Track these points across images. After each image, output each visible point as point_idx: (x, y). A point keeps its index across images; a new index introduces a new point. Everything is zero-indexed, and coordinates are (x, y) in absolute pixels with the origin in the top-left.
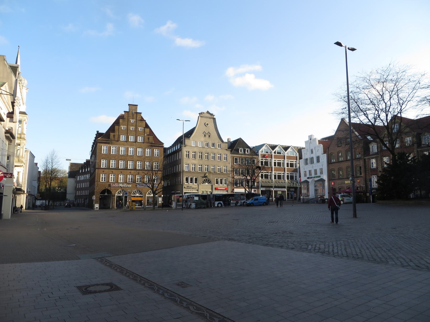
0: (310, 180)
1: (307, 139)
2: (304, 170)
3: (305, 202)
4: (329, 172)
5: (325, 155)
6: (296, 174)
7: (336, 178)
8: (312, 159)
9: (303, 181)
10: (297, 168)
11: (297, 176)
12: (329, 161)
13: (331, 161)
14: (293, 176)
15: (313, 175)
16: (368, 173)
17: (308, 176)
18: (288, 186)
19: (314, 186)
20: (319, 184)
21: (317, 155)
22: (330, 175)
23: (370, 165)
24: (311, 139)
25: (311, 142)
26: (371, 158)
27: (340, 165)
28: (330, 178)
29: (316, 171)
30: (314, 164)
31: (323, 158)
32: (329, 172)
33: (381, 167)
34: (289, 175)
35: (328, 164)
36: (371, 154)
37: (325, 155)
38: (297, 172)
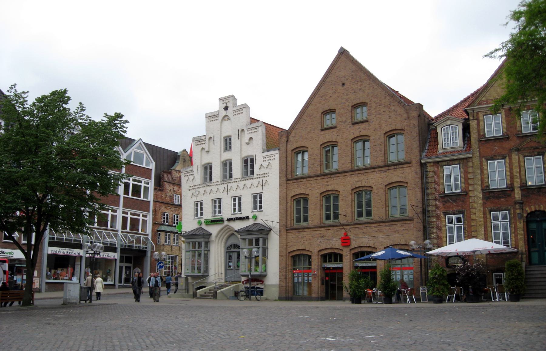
0: (214, 230)
1: (215, 107)
2: (194, 199)
3: (201, 295)
4: (287, 203)
5: (276, 155)
6: (146, 216)
7: (310, 223)
8: (227, 165)
9: (277, 214)
10: (149, 200)
11: (146, 221)
12: (289, 173)
13: (293, 171)
14: (139, 219)
15: (227, 212)
16: (434, 208)
17: (208, 214)
18: (126, 246)
19: (225, 246)
20: (245, 239)
21: (245, 154)
22: (289, 212)
23: (441, 182)
24: (226, 108)
25: (226, 116)
26: (444, 164)
27: (329, 183)
28: (289, 223)
29: (237, 201)
30: (233, 180)
31: (265, 164)
32: (287, 203)
33: (482, 190)
34: (127, 218)
35: (285, 182)
36: (440, 152)
37: (276, 155)
38: (149, 211)
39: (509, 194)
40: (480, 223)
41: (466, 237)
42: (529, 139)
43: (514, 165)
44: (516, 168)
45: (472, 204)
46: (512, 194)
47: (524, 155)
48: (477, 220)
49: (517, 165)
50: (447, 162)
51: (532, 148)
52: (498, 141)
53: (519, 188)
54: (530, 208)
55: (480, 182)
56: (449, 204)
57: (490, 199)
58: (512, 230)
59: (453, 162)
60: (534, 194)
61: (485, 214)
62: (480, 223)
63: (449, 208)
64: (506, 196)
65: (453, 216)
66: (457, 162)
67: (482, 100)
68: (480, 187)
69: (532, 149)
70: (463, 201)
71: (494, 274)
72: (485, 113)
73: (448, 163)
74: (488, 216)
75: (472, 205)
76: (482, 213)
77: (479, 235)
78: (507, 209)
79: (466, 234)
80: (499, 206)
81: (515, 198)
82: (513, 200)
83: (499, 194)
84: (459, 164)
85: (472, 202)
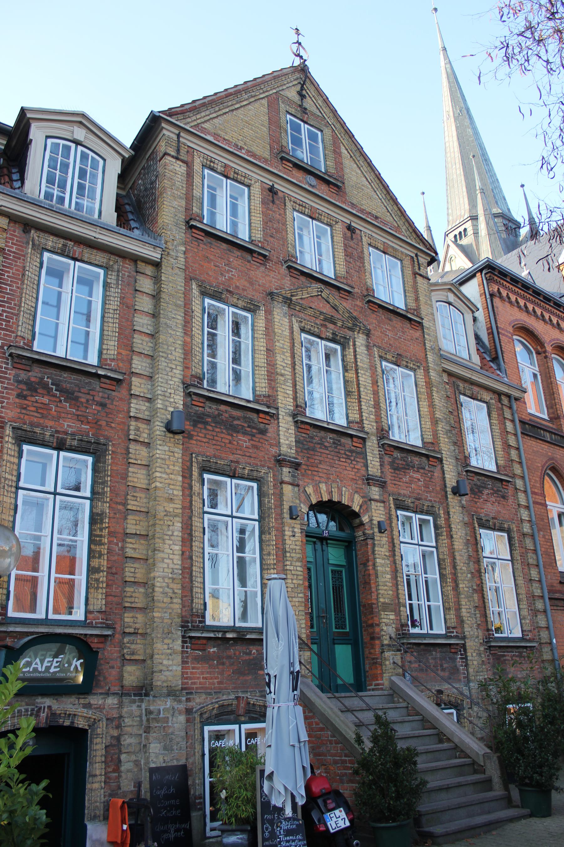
26: (51, 241)
39: (262, 426)
40: (170, 507)
41: (101, 555)
42: (315, 287)
43: (278, 341)
44: (283, 353)
45: (140, 425)
46: (271, 429)
47: (303, 325)
48: (159, 493)
49: (287, 345)
50: (62, 241)
51: (321, 313)
52: (238, 253)
53: (290, 415)
54: (317, 490)
55: (178, 354)
56: (46, 400)
57: (206, 423)
58: (269, 554)
59: (87, 253)
60: (326, 448)
61: (187, 474)
62: (170, 507)
63: (43, 417)
64: (254, 431)
65: (55, 453)
66: (100, 257)
67: (203, 126)
68: (178, 372)
69: (322, 317)
70: (103, 405)
71: (207, 729)
72: (211, 161)
73: (65, 245)
74: (196, 486)
75: (137, 429)
76: (178, 468)
77: (160, 555)
78: (255, 474)
79: (100, 543)
80: (232, 457)
81: (278, 444)
82: (274, 450)
83: (234, 418)
84: (106, 268)
85: (137, 419)
